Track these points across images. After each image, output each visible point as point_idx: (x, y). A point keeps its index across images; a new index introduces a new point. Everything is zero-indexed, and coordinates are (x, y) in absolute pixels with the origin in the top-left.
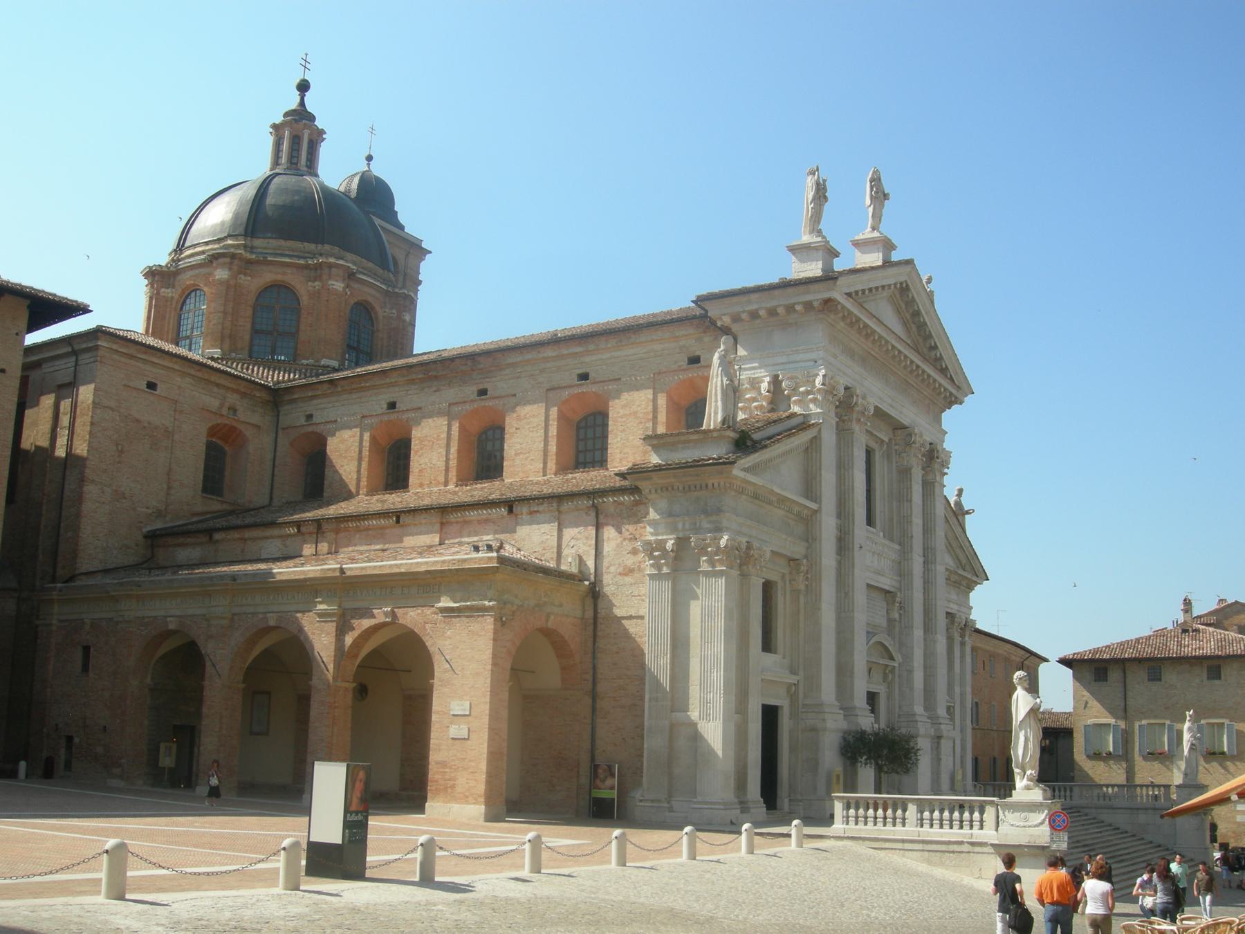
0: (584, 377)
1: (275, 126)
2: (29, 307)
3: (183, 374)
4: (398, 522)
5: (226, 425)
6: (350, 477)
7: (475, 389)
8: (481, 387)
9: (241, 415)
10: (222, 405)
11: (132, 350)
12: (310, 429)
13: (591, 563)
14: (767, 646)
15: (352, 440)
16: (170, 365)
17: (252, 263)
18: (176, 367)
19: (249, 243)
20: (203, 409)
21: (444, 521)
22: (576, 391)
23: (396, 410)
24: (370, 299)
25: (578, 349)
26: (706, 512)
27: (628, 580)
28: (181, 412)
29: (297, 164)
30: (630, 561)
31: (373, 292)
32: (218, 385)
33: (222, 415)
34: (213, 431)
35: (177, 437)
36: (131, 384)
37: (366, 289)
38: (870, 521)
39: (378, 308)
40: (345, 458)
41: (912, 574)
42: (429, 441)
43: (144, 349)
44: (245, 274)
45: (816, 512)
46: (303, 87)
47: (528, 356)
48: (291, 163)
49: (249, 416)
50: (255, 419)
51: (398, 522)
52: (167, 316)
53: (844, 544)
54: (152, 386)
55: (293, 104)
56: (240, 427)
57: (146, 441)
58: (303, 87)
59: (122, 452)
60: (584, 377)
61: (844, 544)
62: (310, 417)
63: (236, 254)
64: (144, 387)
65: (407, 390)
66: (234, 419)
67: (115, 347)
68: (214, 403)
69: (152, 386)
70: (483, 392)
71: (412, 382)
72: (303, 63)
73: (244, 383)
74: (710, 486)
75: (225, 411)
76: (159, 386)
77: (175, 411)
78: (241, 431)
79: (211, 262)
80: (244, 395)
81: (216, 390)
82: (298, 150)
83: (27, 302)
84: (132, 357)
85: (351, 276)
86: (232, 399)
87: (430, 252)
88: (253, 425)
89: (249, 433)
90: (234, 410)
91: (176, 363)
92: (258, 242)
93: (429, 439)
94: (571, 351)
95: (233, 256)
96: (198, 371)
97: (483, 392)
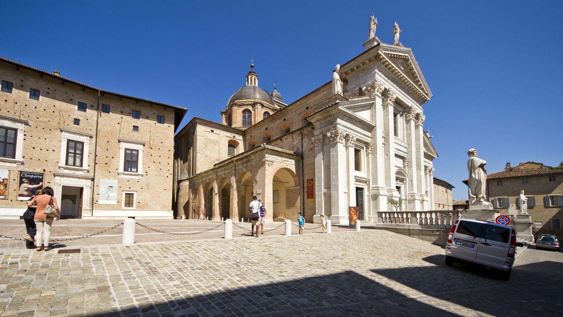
0: (307, 108)
2: (174, 111)
7: (283, 119)
8: (284, 118)
9: (236, 137)
13: (301, 149)
14: (357, 167)
22: (306, 112)
25: (305, 100)
26: (331, 124)
27: (311, 152)
28: (221, 137)
30: (311, 146)
34: (230, 141)
35: (220, 143)
38: (396, 134)
41: (411, 151)
45: (374, 126)
47: (294, 106)
53: (386, 138)
56: (236, 140)
59: (206, 146)
60: (307, 108)
61: (386, 138)
62: (251, 136)
64: (210, 131)
67: (201, 122)
70: (285, 120)
74: (332, 115)
78: (237, 142)
83: (174, 110)
90: (235, 137)
94: (304, 101)
97: (285, 120)
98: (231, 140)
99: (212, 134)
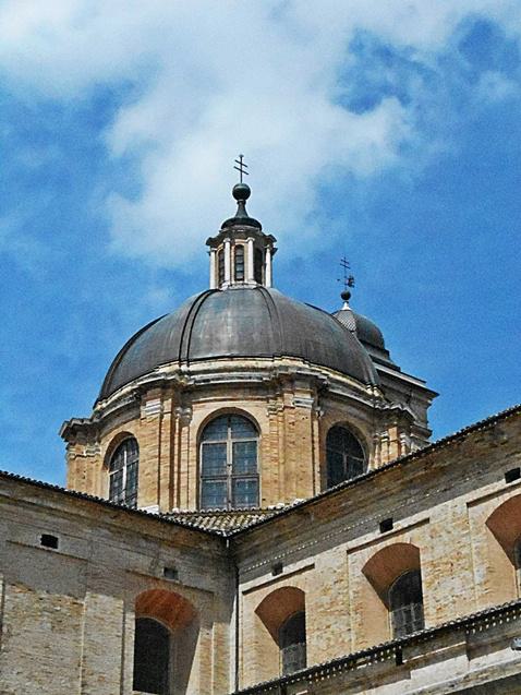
1: (212, 242)
3: (94, 524)
4: (399, 661)
5: (162, 593)
6: (340, 640)
7: (501, 472)
10: (155, 563)
11: (18, 492)
12: (281, 584)
15: (338, 586)
16: (74, 511)
17: (190, 392)
18: (83, 513)
19: (184, 368)
20: (128, 571)
21: (472, 644)
23: (393, 530)
24: (352, 421)
29: (243, 280)
31: (354, 411)
32: (146, 537)
33: (157, 579)
36: (19, 540)
37: (345, 408)
39: (364, 431)
40: (332, 613)
42: (446, 564)
43: (32, 489)
44: (184, 406)
46: (242, 194)
48: (236, 280)
49: (194, 578)
50: (206, 582)
51: (399, 661)
52: (94, 480)
54: (50, 541)
55: (231, 209)
56: (186, 595)
57: (45, 618)
58: (242, 194)
63: (169, 381)
64: (39, 544)
65: (406, 499)
66: (174, 584)
68: (143, 562)
69: (50, 541)
71: (410, 484)
72: (239, 166)
73: (184, 533)
75: (160, 573)
76: (60, 540)
77: (86, 574)
79: (139, 399)
80: (185, 550)
81: (143, 543)
82: (243, 263)
84: (17, 502)
85: (321, 391)
86: (169, 556)
87: (436, 395)
88: (202, 590)
89: (197, 602)
90: (171, 571)
91: (81, 507)
92: (194, 367)
93: (445, 560)
95: (164, 385)
96: (115, 517)
98: (152, 593)
99: (45, 558)
